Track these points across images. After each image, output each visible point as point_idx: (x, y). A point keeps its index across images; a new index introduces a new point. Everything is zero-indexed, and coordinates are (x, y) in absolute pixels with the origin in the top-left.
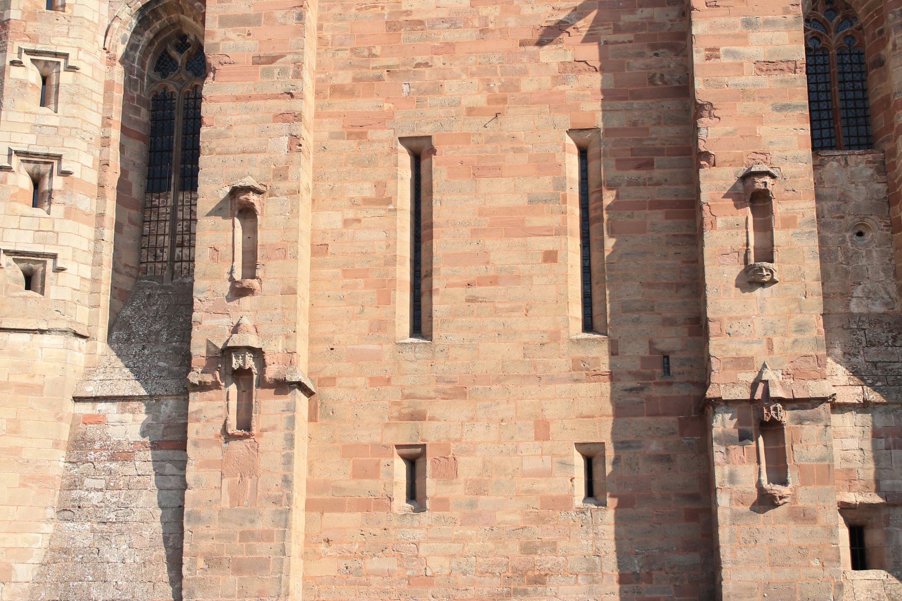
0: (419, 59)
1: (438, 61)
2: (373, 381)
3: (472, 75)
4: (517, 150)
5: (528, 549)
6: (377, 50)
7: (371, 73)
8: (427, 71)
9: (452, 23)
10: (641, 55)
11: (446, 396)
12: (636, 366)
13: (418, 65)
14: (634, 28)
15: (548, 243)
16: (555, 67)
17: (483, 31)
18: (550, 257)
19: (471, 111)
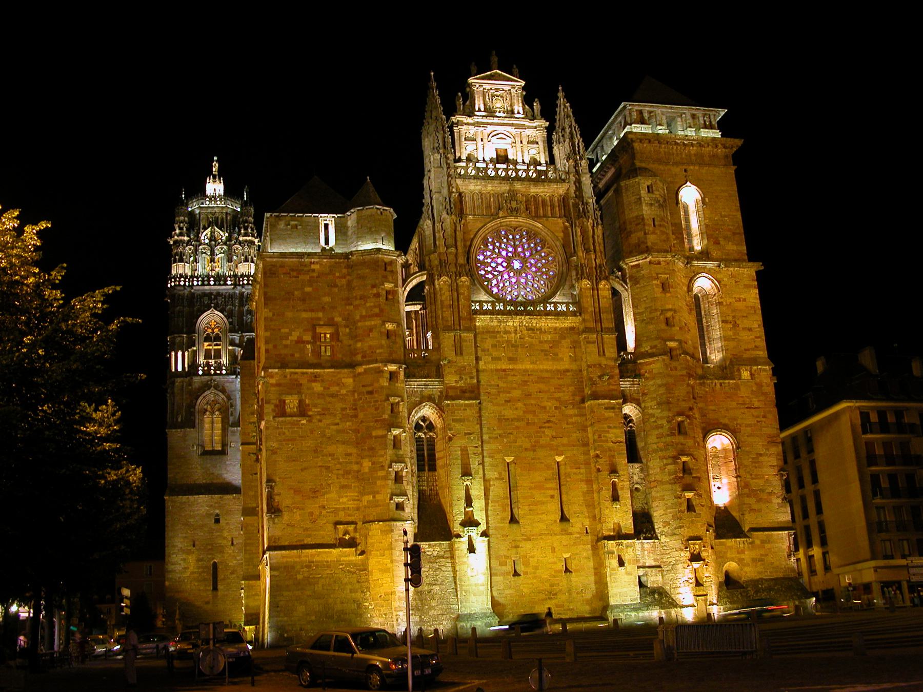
0: (509, 431)
1: (515, 432)
2: (503, 536)
3: (525, 437)
4: (541, 463)
5: (552, 585)
6: (495, 428)
7: (494, 435)
8: (511, 436)
9: (518, 420)
10: (576, 432)
11: (525, 540)
12: (579, 530)
13: (509, 433)
14: (573, 423)
15: (551, 492)
16: (550, 434)
17: (528, 424)
18: (552, 497)
19: (526, 449)
